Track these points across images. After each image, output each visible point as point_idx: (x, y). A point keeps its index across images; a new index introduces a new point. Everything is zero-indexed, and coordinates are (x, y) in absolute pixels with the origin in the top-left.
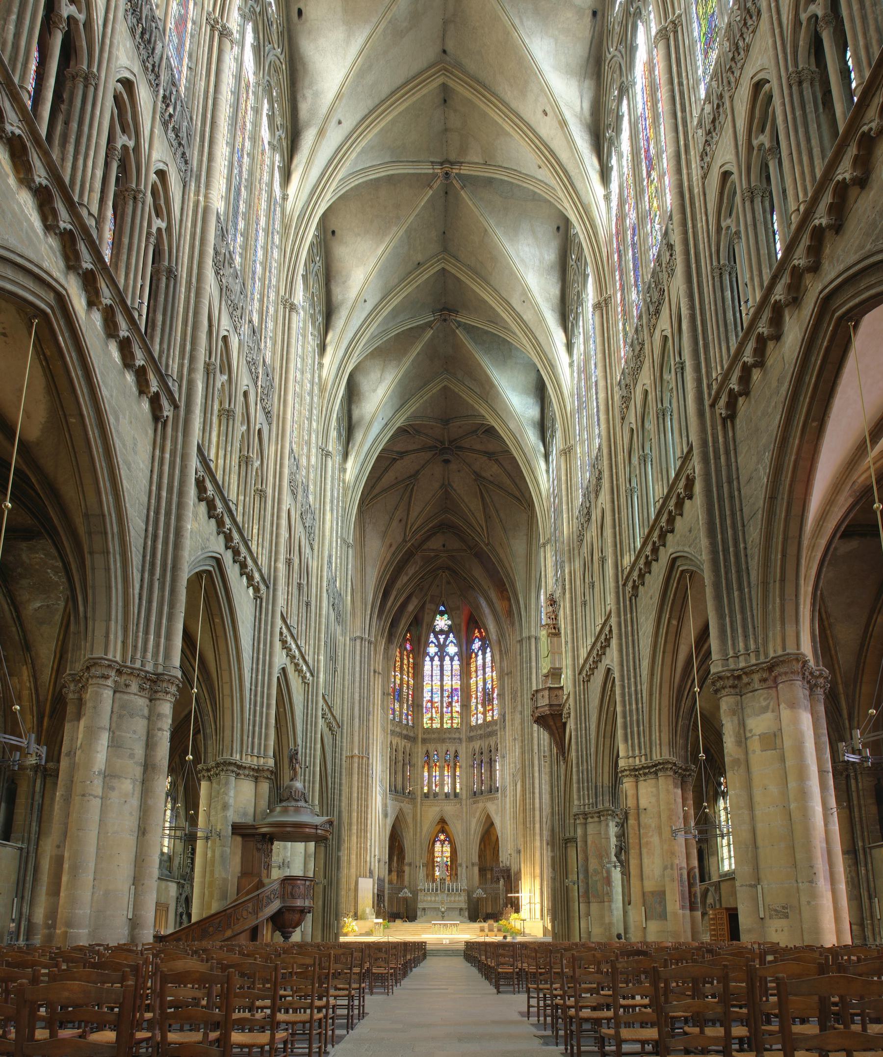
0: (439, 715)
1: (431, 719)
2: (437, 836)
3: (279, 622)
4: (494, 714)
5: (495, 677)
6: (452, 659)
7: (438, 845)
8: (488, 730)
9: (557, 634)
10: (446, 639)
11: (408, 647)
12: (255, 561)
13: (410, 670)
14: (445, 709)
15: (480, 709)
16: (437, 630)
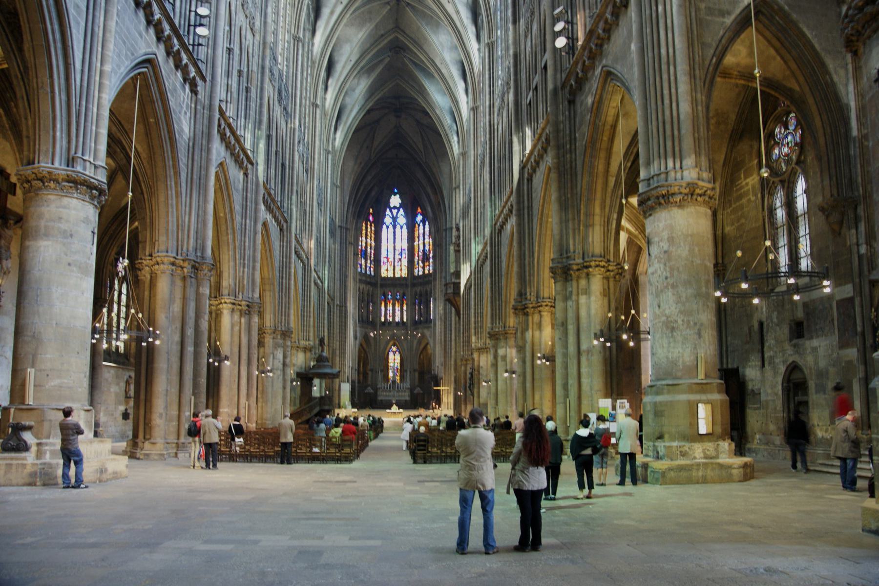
0: (392, 268)
1: (387, 270)
2: (391, 348)
3: (314, 274)
4: (429, 269)
5: (431, 243)
6: (402, 227)
7: (391, 354)
8: (426, 279)
9: (459, 251)
10: (397, 213)
11: (371, 218)
12: (302, 248)
13: (373, 235)
14: (396, 264)
15: (421, 264)
16: (392, 206)
